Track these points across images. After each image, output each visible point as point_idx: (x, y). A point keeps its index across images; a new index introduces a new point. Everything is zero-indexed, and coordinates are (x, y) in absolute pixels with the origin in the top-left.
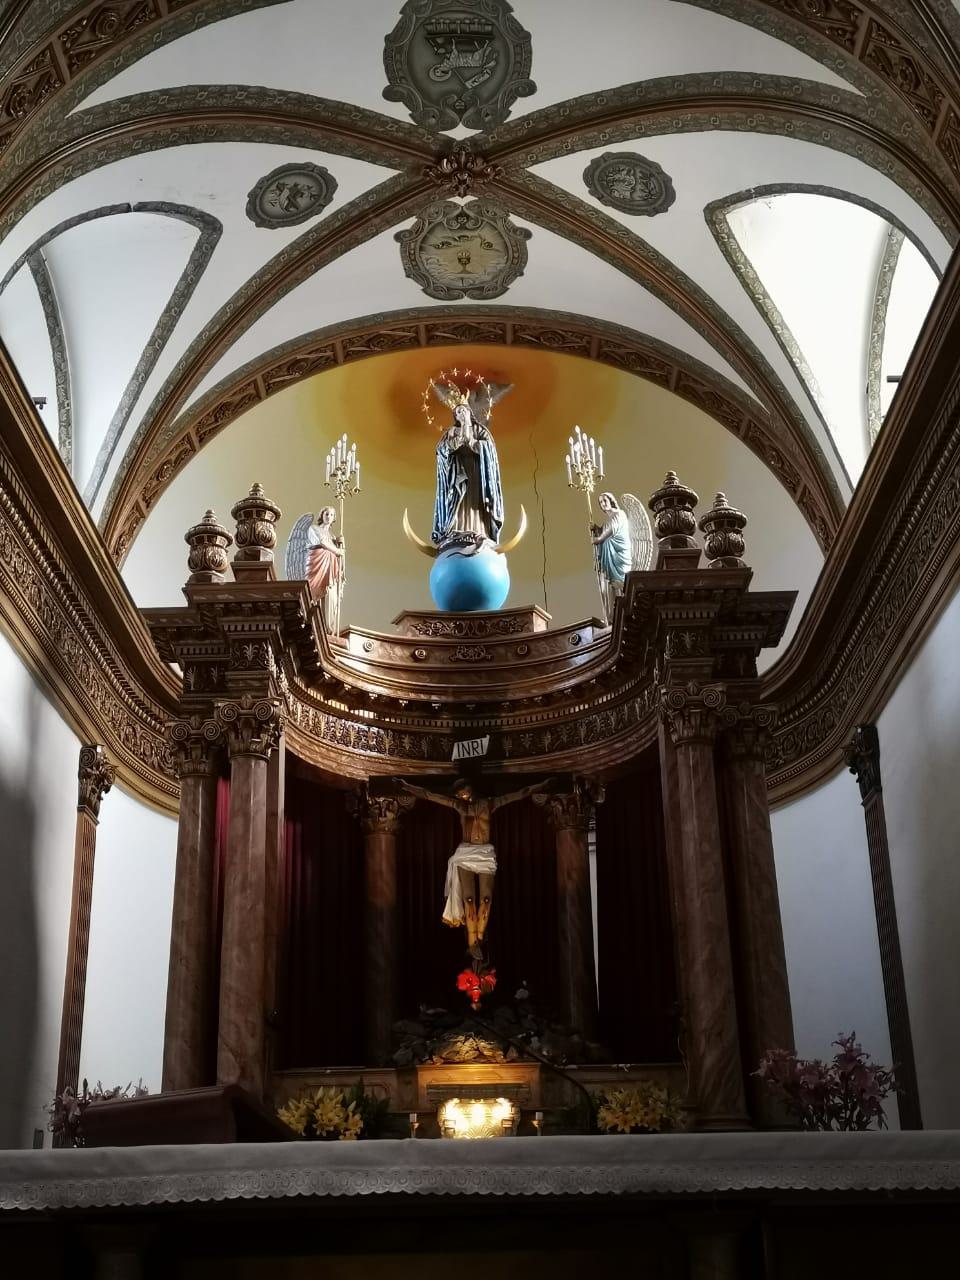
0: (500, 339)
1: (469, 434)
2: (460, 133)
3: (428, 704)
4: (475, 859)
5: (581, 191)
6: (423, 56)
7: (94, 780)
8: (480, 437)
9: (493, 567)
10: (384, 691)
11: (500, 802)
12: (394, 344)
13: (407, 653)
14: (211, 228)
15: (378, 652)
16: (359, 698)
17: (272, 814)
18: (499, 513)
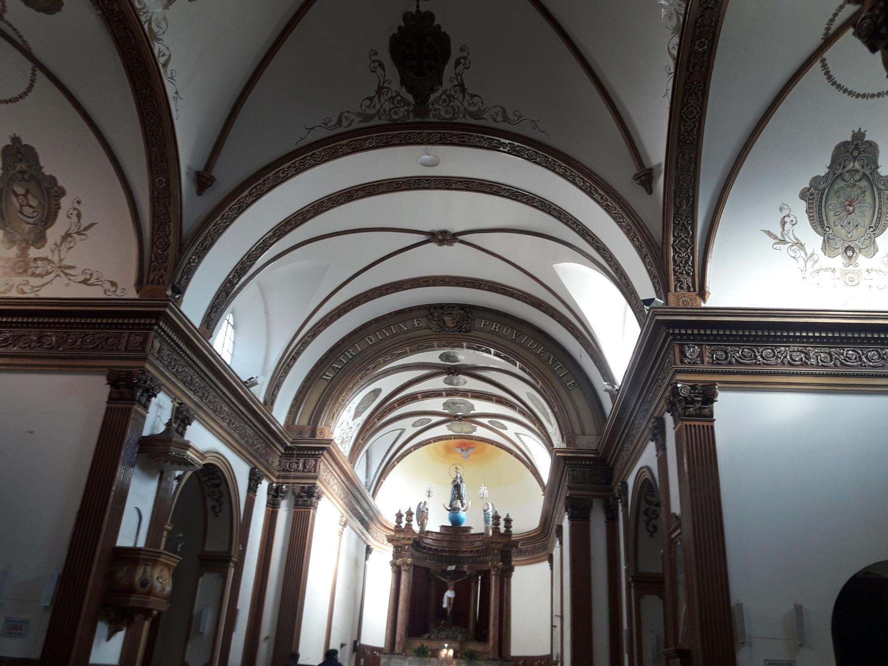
0: (472, 439)
2: (459, 414)
3: (445, 550)
5: (488, 424)
6: (451, 405)
8: (461, 482)
10: (435, 548)
12: (446, 439)
13: (442, 536)
14: (403, 430)
16: (430, 549)
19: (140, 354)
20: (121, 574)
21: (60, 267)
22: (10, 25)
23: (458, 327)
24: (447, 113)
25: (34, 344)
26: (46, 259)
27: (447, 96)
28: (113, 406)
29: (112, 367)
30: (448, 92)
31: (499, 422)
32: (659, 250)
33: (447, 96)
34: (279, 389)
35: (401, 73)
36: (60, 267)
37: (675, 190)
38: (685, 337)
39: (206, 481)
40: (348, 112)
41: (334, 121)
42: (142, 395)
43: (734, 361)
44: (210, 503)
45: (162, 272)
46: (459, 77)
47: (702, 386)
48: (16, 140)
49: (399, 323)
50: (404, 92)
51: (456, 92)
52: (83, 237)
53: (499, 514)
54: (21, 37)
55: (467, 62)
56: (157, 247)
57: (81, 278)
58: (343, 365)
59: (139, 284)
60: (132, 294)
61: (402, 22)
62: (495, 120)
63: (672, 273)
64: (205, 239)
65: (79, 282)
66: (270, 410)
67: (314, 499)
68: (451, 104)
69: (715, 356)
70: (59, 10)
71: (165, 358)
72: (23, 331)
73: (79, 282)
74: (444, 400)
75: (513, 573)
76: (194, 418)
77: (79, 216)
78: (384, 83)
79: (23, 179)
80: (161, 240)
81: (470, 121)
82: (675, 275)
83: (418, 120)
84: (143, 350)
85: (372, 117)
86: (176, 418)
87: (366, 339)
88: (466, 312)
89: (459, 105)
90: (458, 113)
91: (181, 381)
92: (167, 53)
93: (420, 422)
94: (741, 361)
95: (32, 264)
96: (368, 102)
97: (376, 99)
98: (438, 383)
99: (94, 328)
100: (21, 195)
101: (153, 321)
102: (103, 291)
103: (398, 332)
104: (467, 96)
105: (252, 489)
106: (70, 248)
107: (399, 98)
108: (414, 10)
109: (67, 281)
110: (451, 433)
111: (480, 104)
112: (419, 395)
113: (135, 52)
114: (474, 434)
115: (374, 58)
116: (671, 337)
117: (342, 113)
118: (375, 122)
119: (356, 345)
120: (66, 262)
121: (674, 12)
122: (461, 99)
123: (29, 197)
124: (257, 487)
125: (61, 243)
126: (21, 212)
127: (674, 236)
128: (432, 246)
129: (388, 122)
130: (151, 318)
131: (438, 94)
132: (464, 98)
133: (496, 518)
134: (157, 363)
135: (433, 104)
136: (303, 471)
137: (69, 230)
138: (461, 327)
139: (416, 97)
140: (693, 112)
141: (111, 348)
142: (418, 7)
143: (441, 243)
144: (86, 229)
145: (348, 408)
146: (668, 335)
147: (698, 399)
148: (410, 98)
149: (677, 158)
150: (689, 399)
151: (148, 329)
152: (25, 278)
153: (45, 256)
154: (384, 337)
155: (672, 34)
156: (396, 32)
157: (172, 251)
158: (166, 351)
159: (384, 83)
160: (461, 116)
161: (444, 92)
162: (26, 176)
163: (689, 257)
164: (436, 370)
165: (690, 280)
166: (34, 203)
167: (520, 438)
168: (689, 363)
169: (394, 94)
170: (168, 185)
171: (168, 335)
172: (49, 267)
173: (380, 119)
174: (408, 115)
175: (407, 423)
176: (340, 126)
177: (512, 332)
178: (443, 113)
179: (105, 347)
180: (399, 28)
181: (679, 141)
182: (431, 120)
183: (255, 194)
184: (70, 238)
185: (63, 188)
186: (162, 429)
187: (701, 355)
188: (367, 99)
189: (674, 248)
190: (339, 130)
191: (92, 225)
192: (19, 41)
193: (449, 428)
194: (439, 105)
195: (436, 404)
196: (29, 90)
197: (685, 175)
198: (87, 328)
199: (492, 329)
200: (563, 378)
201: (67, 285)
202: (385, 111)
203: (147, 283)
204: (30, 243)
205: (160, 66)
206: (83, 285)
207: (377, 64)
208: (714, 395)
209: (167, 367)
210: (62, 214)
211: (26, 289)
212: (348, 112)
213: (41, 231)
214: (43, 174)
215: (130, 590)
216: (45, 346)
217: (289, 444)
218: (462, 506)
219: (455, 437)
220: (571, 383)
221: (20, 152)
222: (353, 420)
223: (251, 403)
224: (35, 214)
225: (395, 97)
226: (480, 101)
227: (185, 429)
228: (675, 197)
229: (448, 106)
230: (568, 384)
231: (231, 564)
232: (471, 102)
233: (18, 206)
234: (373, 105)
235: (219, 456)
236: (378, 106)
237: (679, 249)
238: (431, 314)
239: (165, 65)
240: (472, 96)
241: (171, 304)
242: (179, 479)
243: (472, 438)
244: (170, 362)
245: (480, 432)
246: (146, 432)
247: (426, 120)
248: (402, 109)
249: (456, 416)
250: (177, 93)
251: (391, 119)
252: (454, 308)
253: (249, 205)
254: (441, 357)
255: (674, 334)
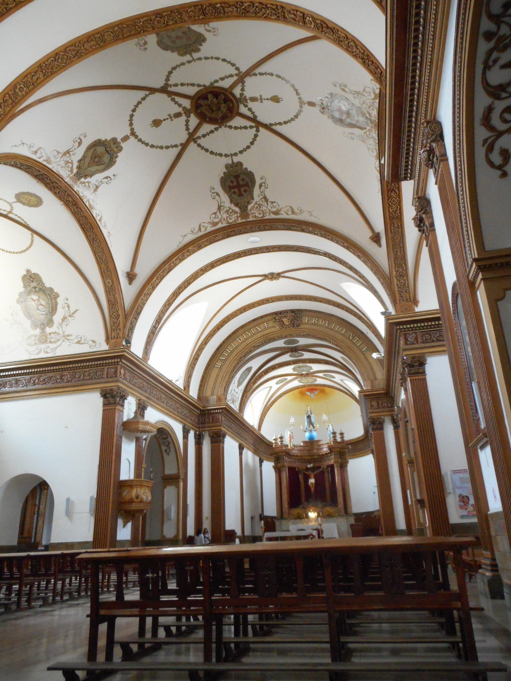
1: (309, 413)
2: (304, 373)
4: (312, 481)
6: (298, 369)
7: (261, 461)
8: (311, 413)
9: (315, 434)
11: (315, 473)
12: (299, 388)
14: (271, 387)
15: (299, 448)
16: (297, 456)
17: (286, 477)
18: (315, 425)
19: (114, 379)
20: (125, 494)
21: (64, 336)
22: (16, 215)
23: (292, 324)
24: (259, 214)
25: (59, 381)
26: (55, 333)
27: (258, 205)
28: (106, 408)
29: (102, 387)
30: (258, 203)
31: (329, 375)
32: (388, 278)
33: (258, 205)
34: (191, 378)
35: (230, 197)
36: (64, 336)
37: (393, 245)
38: (407, 330)
39: (159, 437)
40: (204, 223)
41: (197, 229)
42: (120, 400)
43: (435, 339)
44: (164, 448)
45: (118, 331)
46: (263, 194)
47: (418, 356)
48: (28, 271)
49: (254, 327)
50: (233, 207)
51: (262, 202)
52: (73, 318)
53: (335, 431)
54: (23, 220)
55: (266, 185)
56: (113, 318)
57: (76, 341)
58: (226, 357)
59: (108, 340)
60: (104, 347)
61: (225, 169)
62: (288, 214)
63: (397, 292)
64: (137, 309)
65: (76, 343)
66: (188, 391)
67: (221, 438)
68: (261, 209)
69: (424, 337)
70: (41, 205)
71: (128, 377)
72: (51, 374)
73: (76, 343)
74: (292, 366)
75: (348, 464)
76: (148, 406)
77: (68, 307)
78: (221, 204)
79: (36, 291)
80: (115, 314)
81: (273, 216)
82: (399, 293)
83: (244, 220)
84: (116, 376)
85: (217, 223)
86: (138, 408)
87: (237, 339)
88: (296, 314)
89: (266, 209)
90: (266, 213)
91: (138, 387)
92: (100, 214)
93: (281, 381)
94: (440, 339)
95: (49, 336)
96: (214, 215)
97: (218, 213)
98: (286, 358)
99: (88, 368)
100: (36, 300)
101: (119, 360)
102: (89, 346)
103: (256, 332)
104: (269, 203)
105: (185, 437)
106: (67, 325)
107: (231, 210)
108: (230, 162)
109: (69, 343)
110: (301, 384)
111: (277, 207)
112: (276, 366)
113: (84, 218)
114: (316, 383)
115: (213, 191)
116: (399, 331)
117: (200, 224)
118: (220, 226)
119: (232, 344)
120: (66, 333)
121: (374, 148)
122: (266, 204)
123: (41, 300)
124: (188, 436)
125: (62, 323)
126: (38, 309)
127: (396, 271)
128: (267, 282)
129: (228, 224)
130: (117, 358)
131: (252, 205)
132: (268, 205)
133: (334, 433)
134: (124, 381)
135: (250, 210)
136: (213, 422)
137: (65, 315)
138: (293, 324)
139: (240, 208)
140: (395, 200)
141: (99, 377)
142: (232, 160)
143: (271, 279)
144: (73, 314)
145: (233, 382)
146: (397, 330)
147: (416, 364)
148: (237, 209)
149: (391, 227)
150: (411, 365)
151: (117, 364)
152: (46, 345)
153: (54, 331)
154: (248, 336)
155: (376, 159)
156: (223, 175)
157: (121, 319)
158: (128, 375)
159: (221, 204)
160: (268, 214)
161: (256, 203)
162: (37, 289)
163: (405, 282)
164: (283, 351)
165: (408, 295)
166: (43, 302)
167: (344, 382)
168: (410, 344)
169: (228, 209)
170: (113, 283)
171: (127, 366)
172: (58, 337)
173: (222, 223)
174: (238, 219)
175: (273, 383)
176: (201, 231)
177: (325, 322)
178: (257, 215)
179: (96, 377)
180: (224, 173)
181: (390, 218)
182: (251, 219)
183: (160, 278)
184: (66, 320)
185: (57, 293)
186: (132, 415)
187: (416, 339)
188: (213, 214)
189: (397, 278)
190: (200, 234)
191: (76, 311)
192: (22, 222)
193: (300, 381)
194: (254, 210)
195: (289, 369)
196: (31, 245)
197: (397, 236)
198: (85, 368)
199: (313, 322)
200: (360, 347)
201: (69, 345)
202: (224, 219)
203: (111, 339)
204: (46, 325)
205: (98, 221)
206: (77, 345)
207: (215, 194)
208: (426, 360)
209: (129, 382)
210: (59, 307)
211: (48, 350)
212: (204, 223)
213: (50, 318)
214: (45, 287)
215: (131, 501)
216: (65, 381)
217: (202, 408)
218: (314, 428)
219: (304, 386)
220: (364, 349)
221: (32, 277)
222: (238, 388)
223: (177, 391)
224: (45, 309)
225: (229, 210)
226: (277, 204)
227: (144, 412)
228: (393, 249)
229: (259, 210)
230: (363, 350)
231: (181, 480)
232: (272, 206)
233: (36, 306)
234: (217, 216)
235: (164, 423)
236: (220, 217)
237: (400, 278)
238: (274, 318)
239: (100, 220)
240: (272, 203)
241: (126, 350)
242: (145, 439)
243: (316, 385)
244: (131, 379)
245: (319, 381)
246: (125, 419)
247: (248, 220)
248: (233, 216)
249: (302, 375)
250: (109, 233)
251: (228, 222)
252: (287, 312)
253: (157, 285)
254: (285, 343)
255: (400, 329)
